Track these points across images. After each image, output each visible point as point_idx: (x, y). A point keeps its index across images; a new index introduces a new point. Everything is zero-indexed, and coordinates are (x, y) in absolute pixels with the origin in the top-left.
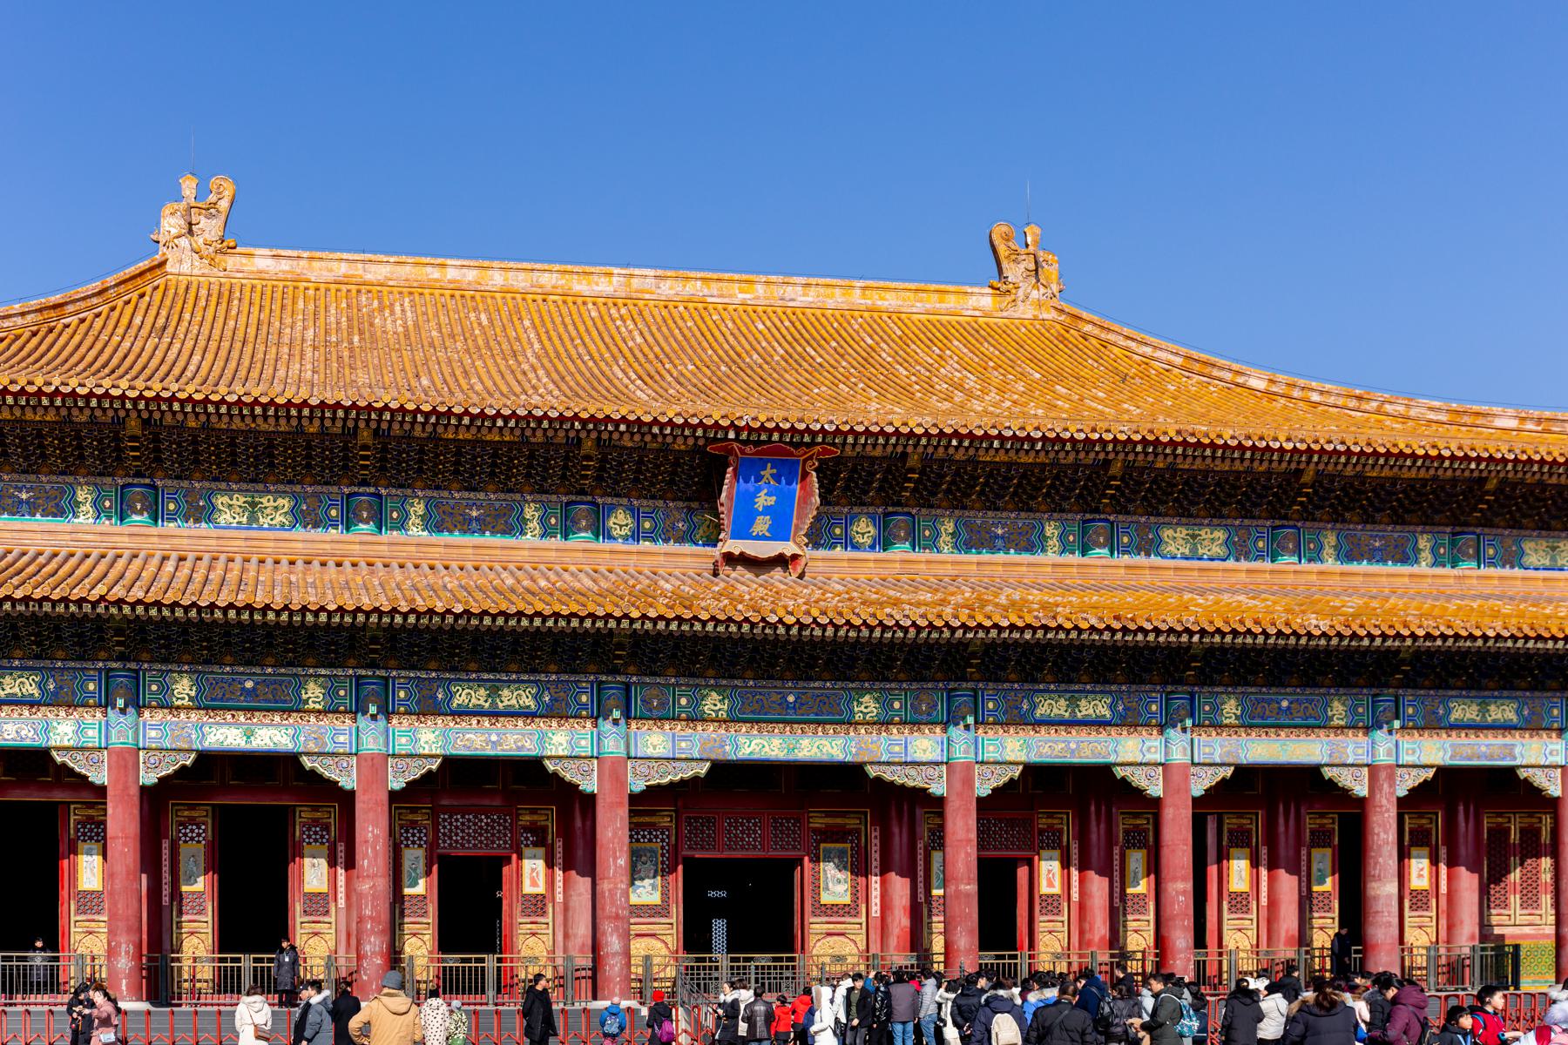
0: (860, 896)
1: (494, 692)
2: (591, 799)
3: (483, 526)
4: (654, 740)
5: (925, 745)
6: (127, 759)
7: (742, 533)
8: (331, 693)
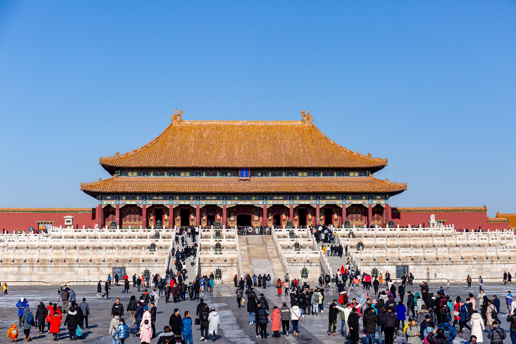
0: (259, 219)
1: (211, 197)
2: (222, 209)
3: (212, 175)
4: (229, 202)
5: (260, 202)
6: (171, 206)
7: (242, 176)
8: (193, 198)
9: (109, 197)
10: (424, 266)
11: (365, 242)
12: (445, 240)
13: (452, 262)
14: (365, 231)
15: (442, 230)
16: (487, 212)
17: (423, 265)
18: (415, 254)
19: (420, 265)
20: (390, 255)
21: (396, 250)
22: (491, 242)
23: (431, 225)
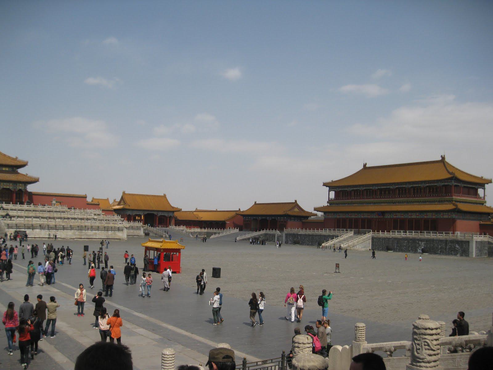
11: (11, 213)
12: (61, 214)
13: (64, 228)
14: (11, 206)
15: (59, 208)
16: (87, 198)
17: (47, 229)
18: (42, 222)
19: (45, 229)
20: (26, 223)
21: (30, 219)
22: (89, 217)
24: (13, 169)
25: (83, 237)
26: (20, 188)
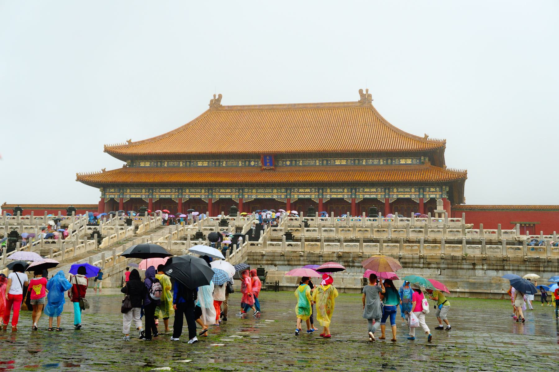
9: (112, 190)
10: (360, 269)
18: (346, 250)
19: (353, 266)
23: (437, 215)
24: (420, 159)
25: (458, 290)
26: (432, 196)
